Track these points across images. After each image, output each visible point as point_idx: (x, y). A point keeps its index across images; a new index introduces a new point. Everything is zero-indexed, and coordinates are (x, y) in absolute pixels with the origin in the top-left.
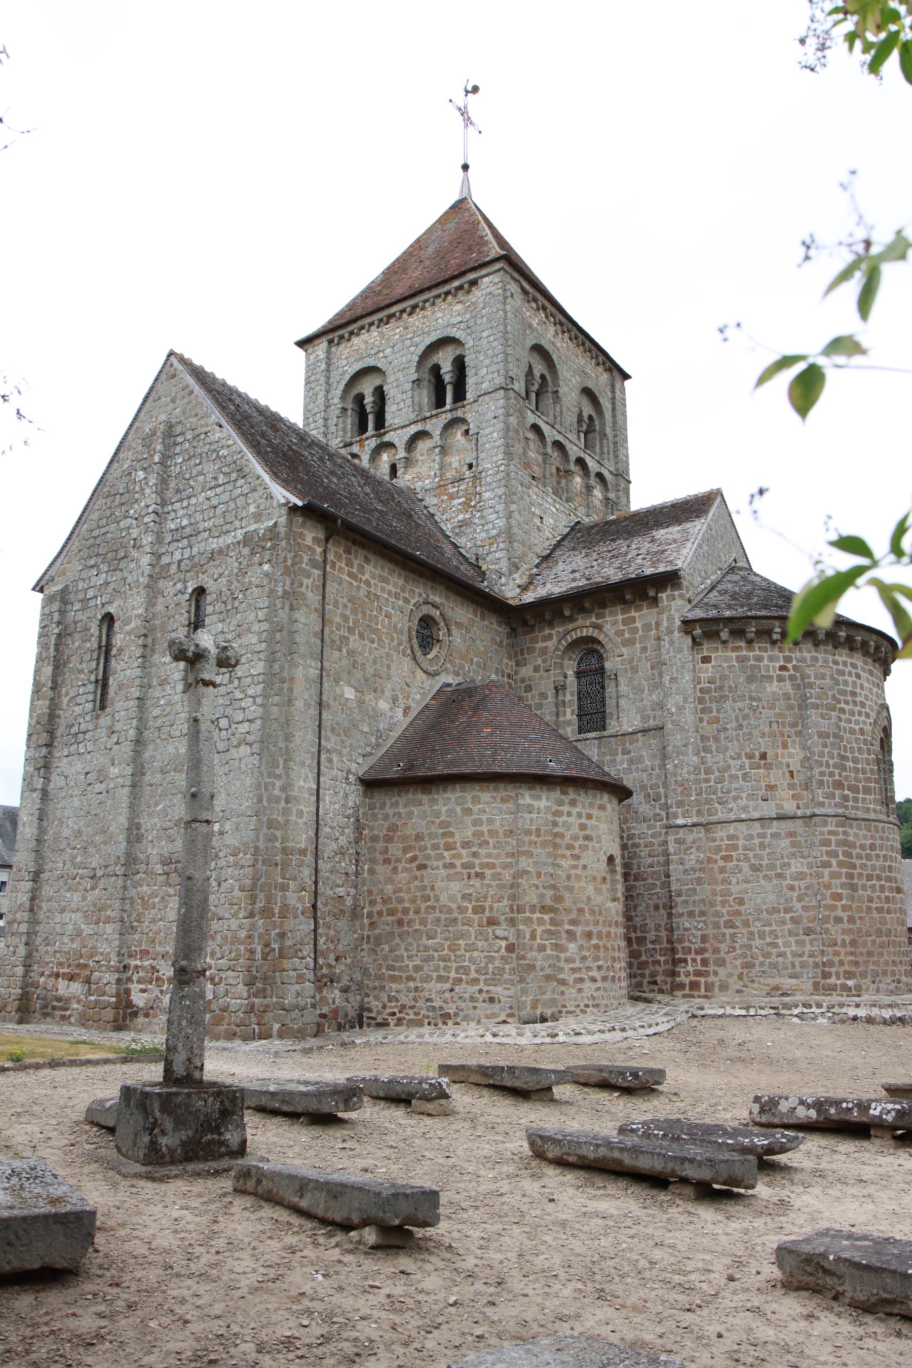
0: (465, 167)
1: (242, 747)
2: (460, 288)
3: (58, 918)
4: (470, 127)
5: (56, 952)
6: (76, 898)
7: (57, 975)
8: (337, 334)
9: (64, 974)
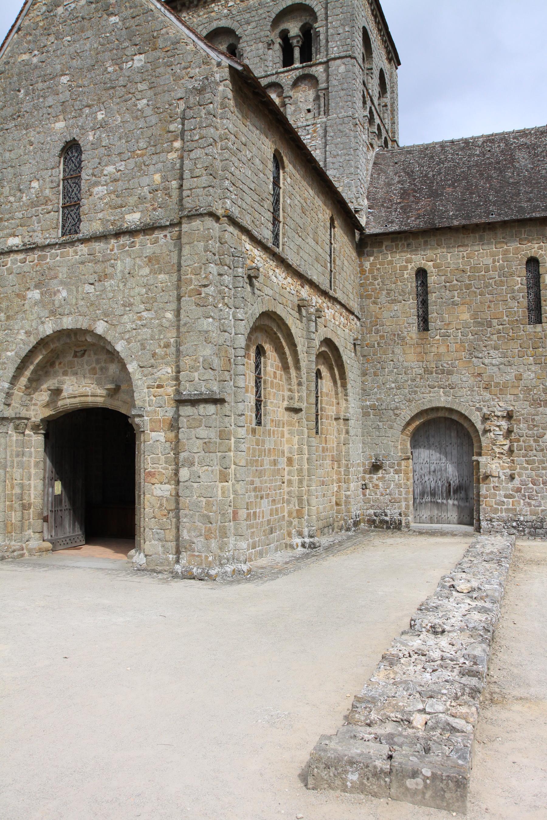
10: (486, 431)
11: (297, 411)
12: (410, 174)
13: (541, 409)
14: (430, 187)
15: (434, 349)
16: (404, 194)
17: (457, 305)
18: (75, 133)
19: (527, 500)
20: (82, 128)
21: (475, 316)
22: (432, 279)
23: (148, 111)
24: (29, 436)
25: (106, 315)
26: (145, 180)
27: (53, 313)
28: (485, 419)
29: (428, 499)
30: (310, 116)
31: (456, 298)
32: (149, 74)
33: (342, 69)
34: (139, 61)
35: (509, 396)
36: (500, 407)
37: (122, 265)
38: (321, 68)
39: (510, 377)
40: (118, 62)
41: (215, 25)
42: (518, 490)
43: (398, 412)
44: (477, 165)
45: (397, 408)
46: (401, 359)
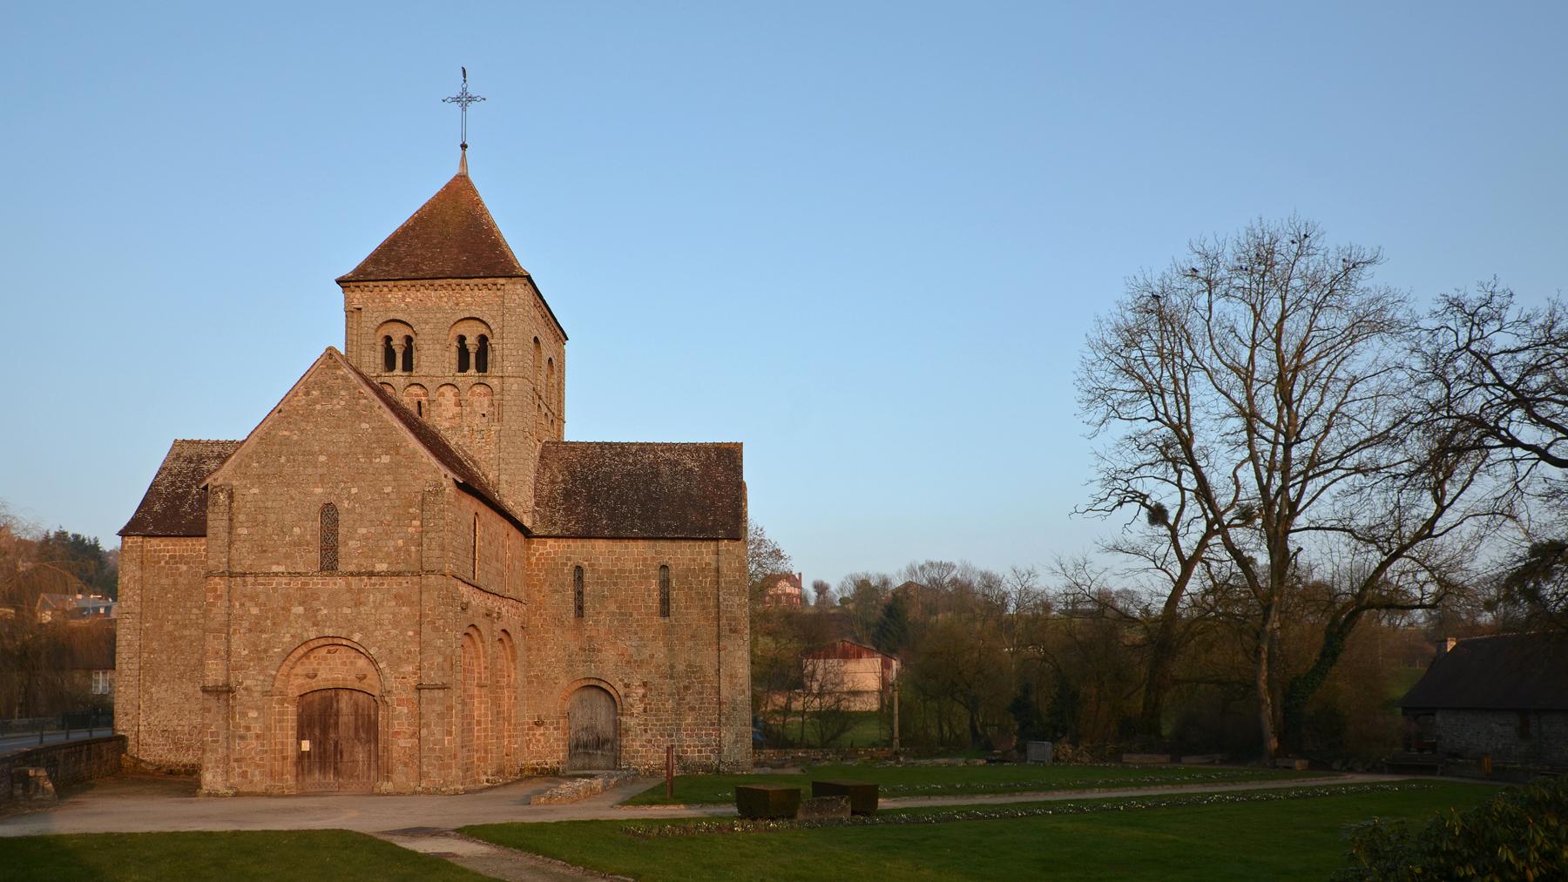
0: (464, 146)
4: (456, 106)
12: (573, 474)
14: (589, 491)
16: (567, 494)
18: (333, 499)
20: (338, 496)
21: (619, 608)
22: (587, 576)
23: (393, 496)
25: (361, 629)
26: (391, 543)
27: (315, 624)
30: (485, 420)
32: (393, 468)
33: (515, 387)
34: (386, 459)
38: (496, 381)
40: (369, 454)
41: (392, 316)
44: (628, 474)
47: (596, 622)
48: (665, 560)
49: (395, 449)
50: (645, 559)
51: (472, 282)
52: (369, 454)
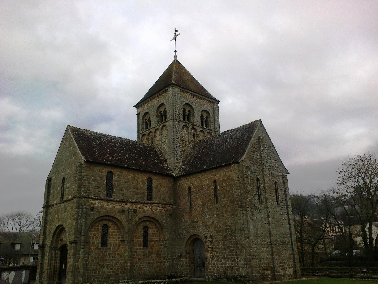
0: (176, 51)
1: (291, 220)
2: (210, 101)
3: (261, 254)
4: (174, 40)
5: (263, 263)
6: (264, 249)
7: (264, 269)
8: (183, 89)
9: (266, 269)
10: (206, 242)
11: (124, 241)
13: (219, 234)
15: (193, 214)
17: (198, 198)
19: (217, 268)
21: (202, 202)
24: (57, 252)
26: (72, 188)
28: (206, 237)
29: (198, 268)
31: (198, 196)
35: (211, 230)
36: (208, 234)
37: (68, 209)
39: (211, 223)
42: (214, 264)
43: (185, 237)
45: (185, 236)
46: (185, 218)
47: (195, 209)
48: (215, 177)
49: (75, 154)
50: (209, 179)
51: (160, 92)
52: (71, 158)
